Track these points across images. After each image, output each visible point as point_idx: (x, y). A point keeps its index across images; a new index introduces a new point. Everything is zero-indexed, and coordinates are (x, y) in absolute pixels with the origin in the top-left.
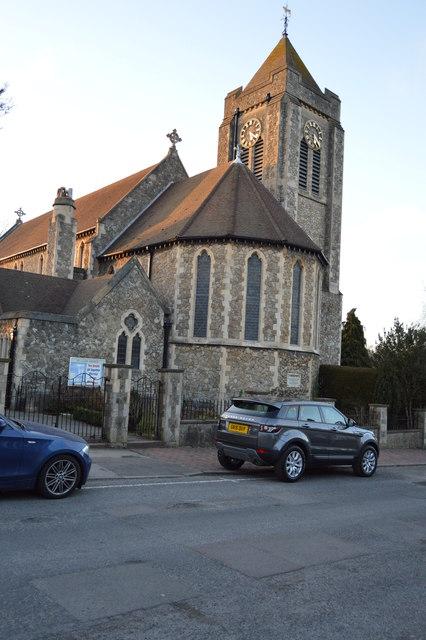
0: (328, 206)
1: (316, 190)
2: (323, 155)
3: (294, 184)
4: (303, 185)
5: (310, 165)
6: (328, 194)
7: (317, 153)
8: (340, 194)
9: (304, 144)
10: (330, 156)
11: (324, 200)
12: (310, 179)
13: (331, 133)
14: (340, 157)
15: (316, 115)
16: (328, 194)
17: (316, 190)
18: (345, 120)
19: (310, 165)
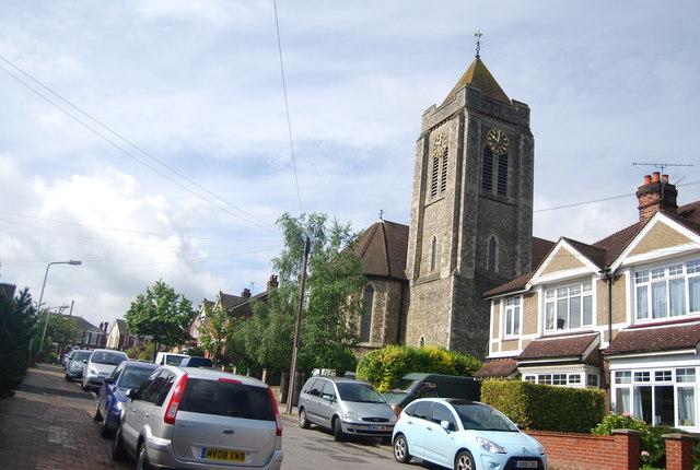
0: (515, 206)
1: (502, 189)
2: (510, 161)
3: (477, 189)
4: (487, 185)
5: (495, 173)
6: (515, 195)
7: (503, 159)
8: (529, 195)
9: (488, 152)
11: (511, 200)
12: (495, 182)
14: (529, 161)
15: (502, 125)
17: (502, 189)
18: (534, 126)
19: (495, 173)
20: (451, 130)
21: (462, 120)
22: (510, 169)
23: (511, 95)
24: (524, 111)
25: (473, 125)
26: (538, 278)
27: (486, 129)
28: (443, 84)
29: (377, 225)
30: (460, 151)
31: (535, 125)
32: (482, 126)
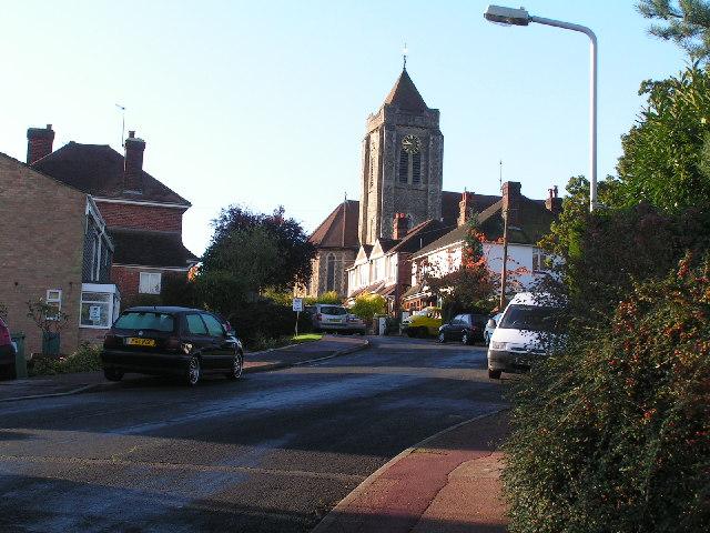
1: (416, 178)
2: (423, 157)
5: (411, 168)
6: (426, 182)
7: (416, 157)
9: (403, 151)
10: (427, 155)
11: (423, 186)
13: (426, 140)
16: (426, 182)
19: (411, 168)
20: (375, 138)
21: (382, 134)
22: (422, 163)
23: (430, 105)
24: (436, 112)
25: (389, 137)
26: (357, 263)
27: (399, 138)
28: (385, 90)
29: (342, 205)
30: (380, 158)
31: (443, 126)
32: (398, 135)
